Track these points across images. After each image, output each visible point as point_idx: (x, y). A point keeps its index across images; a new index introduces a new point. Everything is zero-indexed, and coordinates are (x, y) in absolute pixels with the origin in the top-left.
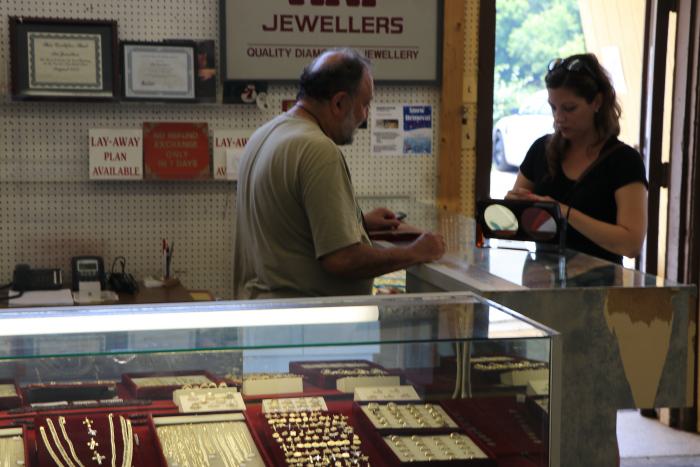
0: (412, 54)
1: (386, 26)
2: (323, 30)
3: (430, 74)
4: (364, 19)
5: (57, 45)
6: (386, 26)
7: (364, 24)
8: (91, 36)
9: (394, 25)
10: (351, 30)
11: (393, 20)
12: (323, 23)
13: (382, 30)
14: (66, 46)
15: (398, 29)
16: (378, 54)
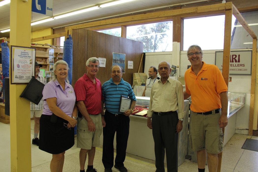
2: (231, 66)
3: (250, 74)
4: (238, 64)
6: (242, 66)
7: (238, 65)
9: (243, 65)
10: (236, 66)
12: (231, 65)
13: (241, 66)
16: (240, 70)
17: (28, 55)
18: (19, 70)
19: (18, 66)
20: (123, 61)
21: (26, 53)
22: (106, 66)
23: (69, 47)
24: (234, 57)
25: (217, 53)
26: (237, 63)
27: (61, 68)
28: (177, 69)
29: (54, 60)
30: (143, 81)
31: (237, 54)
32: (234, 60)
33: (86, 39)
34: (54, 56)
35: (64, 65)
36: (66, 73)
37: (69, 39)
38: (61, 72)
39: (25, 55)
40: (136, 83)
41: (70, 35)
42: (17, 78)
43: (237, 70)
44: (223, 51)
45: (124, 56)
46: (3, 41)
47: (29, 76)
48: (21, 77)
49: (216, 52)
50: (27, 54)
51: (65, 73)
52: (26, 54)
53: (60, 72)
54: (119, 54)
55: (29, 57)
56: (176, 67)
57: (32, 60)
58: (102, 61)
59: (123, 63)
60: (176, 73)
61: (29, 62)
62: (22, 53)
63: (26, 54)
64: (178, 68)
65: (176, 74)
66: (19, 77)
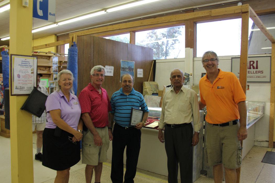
0: (264, 77)
7: (256, 72)
9: (262, 72)
12: (248, 72)
16: (258, 77)
17: (29, 64)
18: (20, 80)
19: (19, 76)
20: (132, 69)
21: (27, 62)
22: (113, 75)
23: (74, 55)
24: (252, 63)
25: (233, 59)
26: (255, 70)
27: (65, 78)
28: (190, 76)
29: (58, 68)
30: (153, 90)
31: (255, 60)
32: (252, 67)
33: (92, 46)
34: (58, 65)
35: (69, 75)
36: (71, 84)
37: (74, 46)
38: (65, 83)
39: (26, 64)
40: (147, 93)
41: (75, 42)
42: (18, 89)
43: (255, 77)
44: (240, 56)
45: (133, 64)
46: (4, 50)
47: (30, 86)
48: (21, 88)
49: (232, 58)
50: (28, 63)
51: (70, 84)
52: (27, 63)
53: (64, 82)
54: (127, 62)
55: (30, 66)
56: (189, 75)
57: (33, 69)
58: (110, 69)
59: (132, 71)
60: (189, 81)
61: (30, 72)
62: (22, 62)
63: (27, 63)
64: (191, 76)
65: (189, 83)
66: (19, 88)
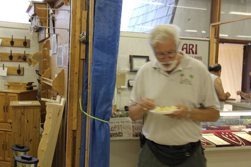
1: (199, 59)
5: (138, 61)
6: (199, 59)
8: (144, 59)
11: (200, 57)
14: (140, 61)
15: (201, 59)
24: (191, 47)
26: (194, 55)
31: (194, 43)
32: (191, 51)
